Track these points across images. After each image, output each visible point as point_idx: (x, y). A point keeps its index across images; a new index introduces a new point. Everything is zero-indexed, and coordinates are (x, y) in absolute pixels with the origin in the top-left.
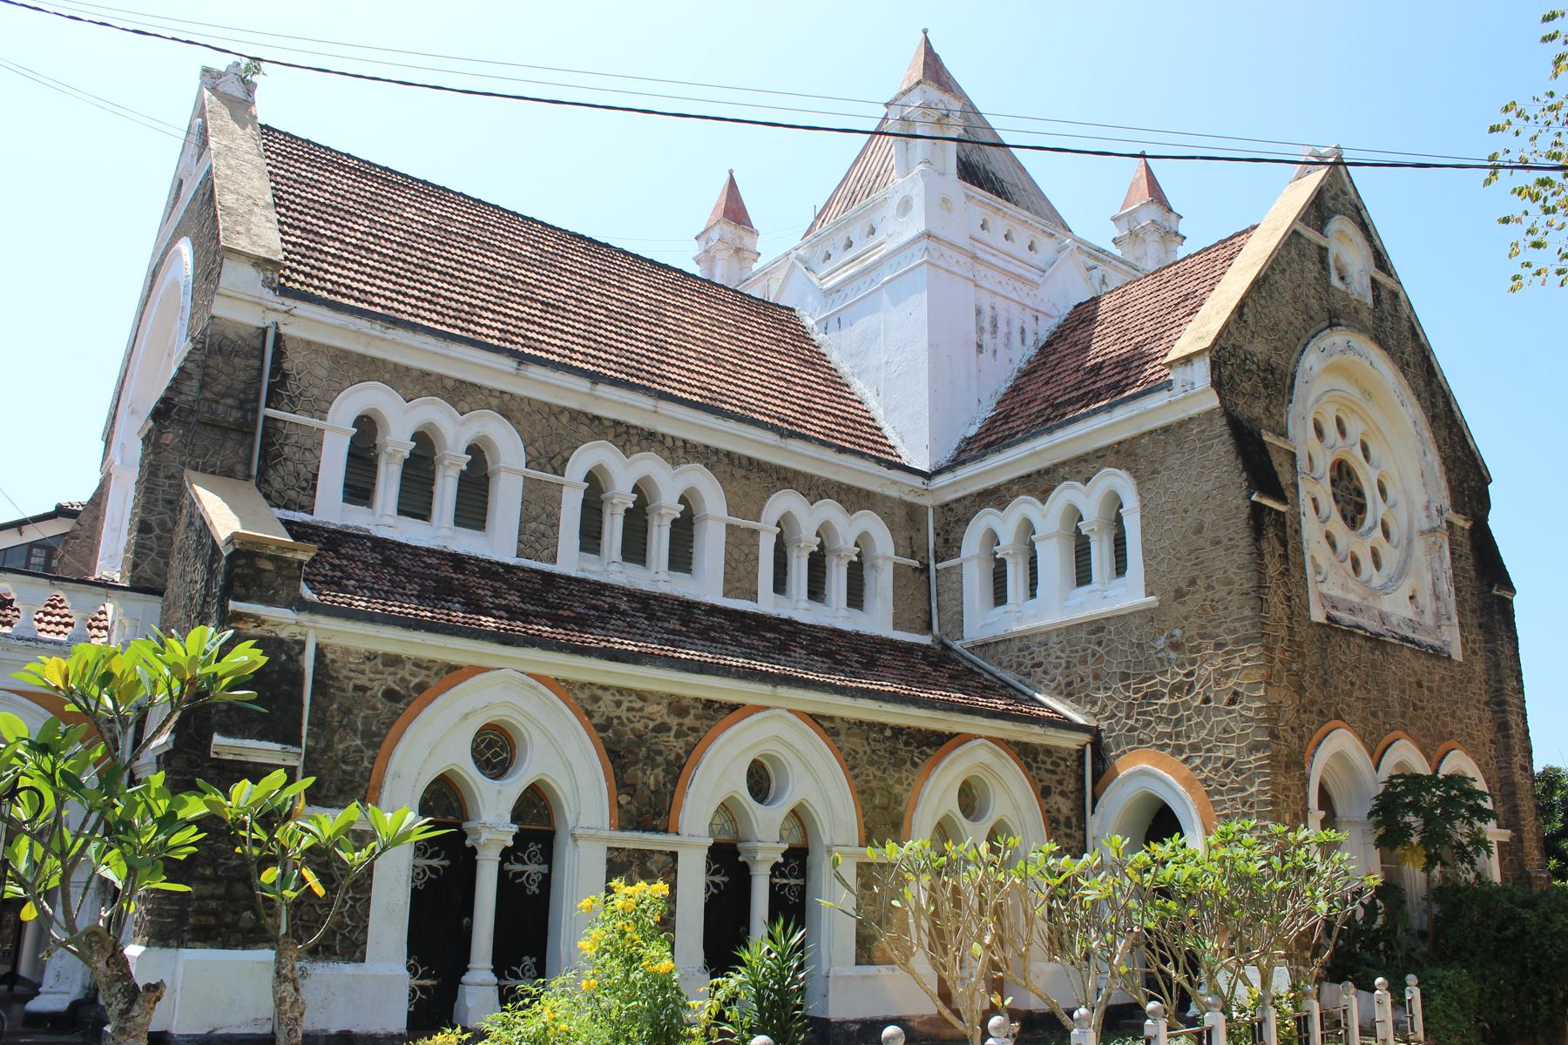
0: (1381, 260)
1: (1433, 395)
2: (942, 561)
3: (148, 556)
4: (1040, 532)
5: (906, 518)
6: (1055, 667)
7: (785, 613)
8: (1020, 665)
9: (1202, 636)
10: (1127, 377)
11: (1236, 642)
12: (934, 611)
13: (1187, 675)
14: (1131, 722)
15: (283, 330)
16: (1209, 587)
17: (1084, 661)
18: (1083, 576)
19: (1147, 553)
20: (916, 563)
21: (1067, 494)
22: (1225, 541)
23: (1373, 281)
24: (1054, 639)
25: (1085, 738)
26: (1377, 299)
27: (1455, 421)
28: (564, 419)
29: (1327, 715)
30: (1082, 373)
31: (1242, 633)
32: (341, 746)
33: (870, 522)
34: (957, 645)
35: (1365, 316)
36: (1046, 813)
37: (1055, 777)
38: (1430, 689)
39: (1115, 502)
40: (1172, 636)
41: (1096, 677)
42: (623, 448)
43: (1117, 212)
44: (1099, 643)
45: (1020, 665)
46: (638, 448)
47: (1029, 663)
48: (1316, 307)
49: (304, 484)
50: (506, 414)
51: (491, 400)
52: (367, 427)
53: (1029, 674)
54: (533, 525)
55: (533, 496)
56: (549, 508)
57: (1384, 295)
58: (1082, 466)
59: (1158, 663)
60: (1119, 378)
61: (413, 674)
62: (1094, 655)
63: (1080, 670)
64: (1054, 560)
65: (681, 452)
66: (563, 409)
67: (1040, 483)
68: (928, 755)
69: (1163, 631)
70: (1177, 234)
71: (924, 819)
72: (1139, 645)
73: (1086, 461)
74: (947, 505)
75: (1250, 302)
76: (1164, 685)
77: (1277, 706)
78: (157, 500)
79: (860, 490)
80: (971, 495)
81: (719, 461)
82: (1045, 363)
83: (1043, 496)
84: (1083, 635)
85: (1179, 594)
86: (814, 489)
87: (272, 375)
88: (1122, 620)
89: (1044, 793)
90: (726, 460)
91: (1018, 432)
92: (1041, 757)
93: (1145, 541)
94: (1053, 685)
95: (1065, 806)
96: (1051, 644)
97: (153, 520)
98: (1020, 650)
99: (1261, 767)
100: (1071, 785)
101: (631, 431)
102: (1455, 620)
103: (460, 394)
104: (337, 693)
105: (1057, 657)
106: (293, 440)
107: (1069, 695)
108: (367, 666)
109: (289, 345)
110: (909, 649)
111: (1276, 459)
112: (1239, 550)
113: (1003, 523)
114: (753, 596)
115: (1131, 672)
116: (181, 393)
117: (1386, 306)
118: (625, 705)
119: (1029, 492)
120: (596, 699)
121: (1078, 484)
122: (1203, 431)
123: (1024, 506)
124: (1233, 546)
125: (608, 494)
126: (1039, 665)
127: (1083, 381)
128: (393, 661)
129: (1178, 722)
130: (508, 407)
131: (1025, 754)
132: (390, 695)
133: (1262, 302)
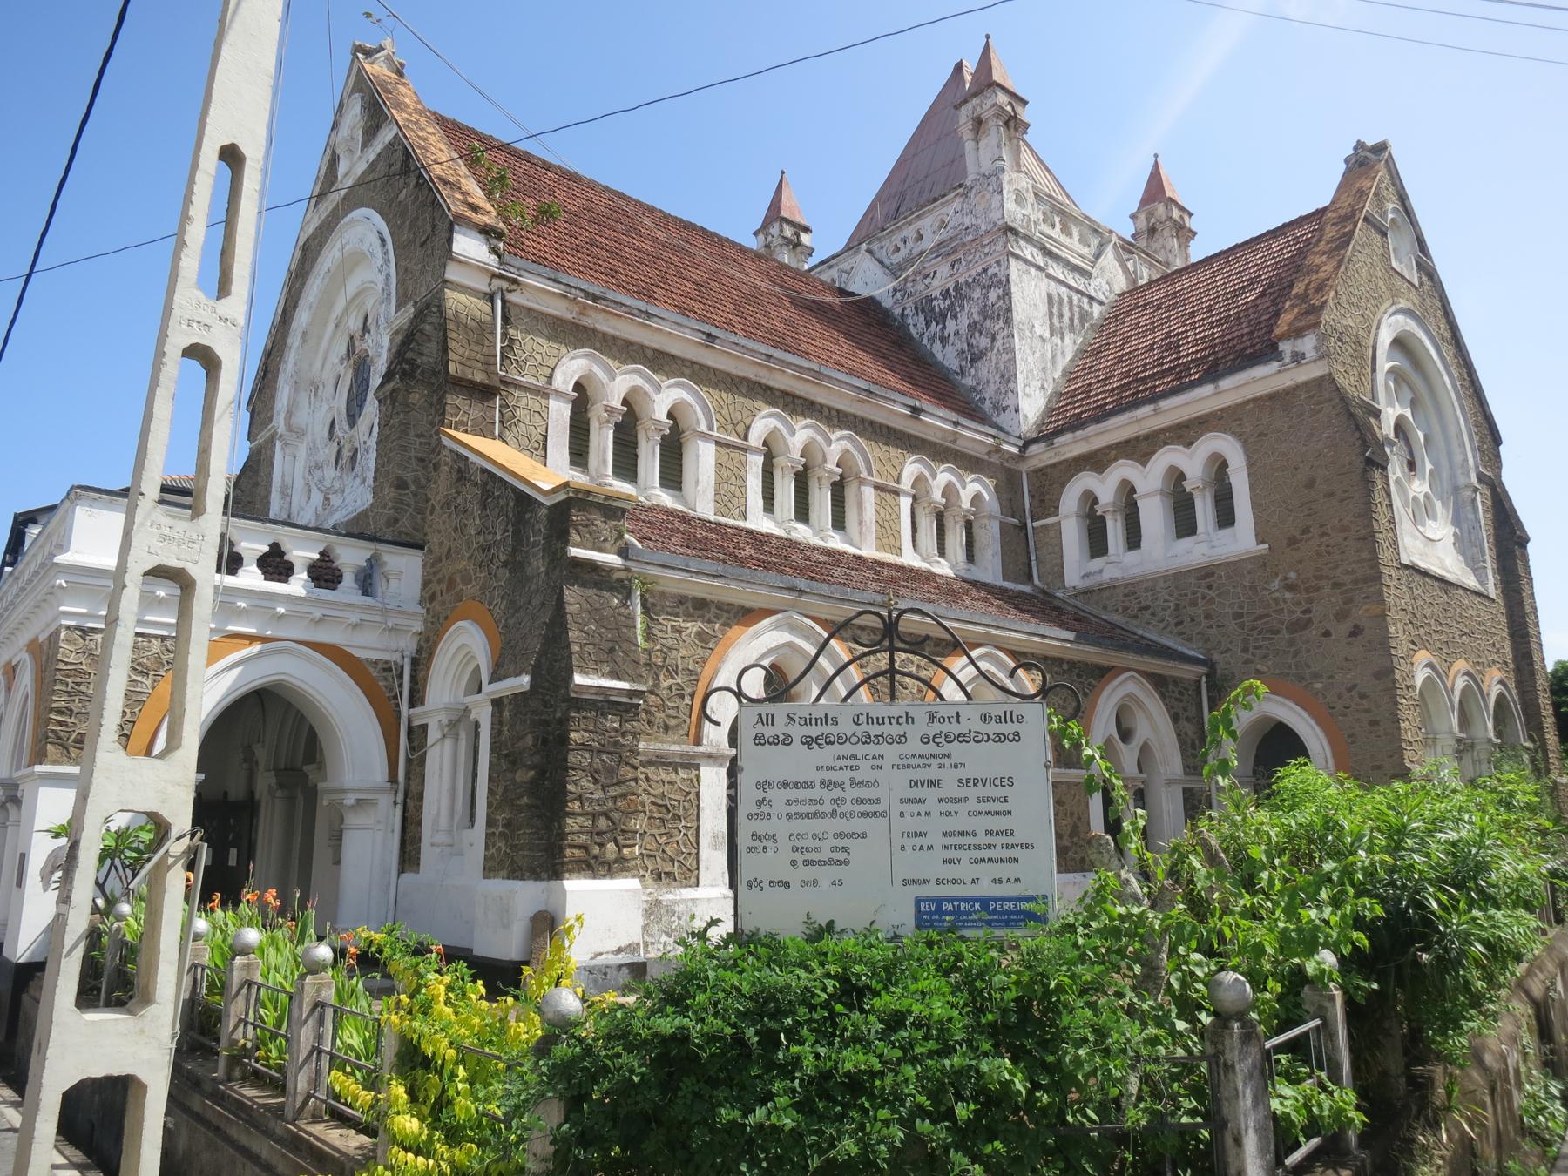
3: (406, 511)
4: (1141, 488)
5: (1008, 483)
6: (1164, 609)
7: (924, 566)
8: (1126, 609)
9: (1320, 578)
11: (1355, 582)
12: (1034, 563)
13: (1304, 612)
14: (1246, 656)
15: (509, 297)
17: (1194, 603)
18: (1185, 525)
19: (1257, 506)
20: (1015, 521)
24: (1162, 585)
25: (1203, 670)
36: (1178, 735)
37: (1181, 705)
39: (1219, 467)
40: (1286, 579)
44: (1210, 587)
47: (1134, 605)
48: (1384, 288)
49: (536, 445)
51: (684, 369)
53: (1136, 617)
58: (1185, 433)
59: (1273, 604)
64: (1154, 515)
65: (836, 420)
66: (743, 379)
67: (1140, 449)
68: (1094, 687)
69: (1277, 575)
70: (1190, 231)
72: (1253, 589)
74: (1041, 470)
78: (410, 458)
79: (971, 456)
80: (1066, 460)
81: (865, 429)
83: (1143, 458)
84: (1193, 580)
85: (1292, 542)
87: (502, 342)
88: (1233, 568)
89: (1175, 719)
90: (870, 430)
92: (1171, 687)
94: (1162, 625)
95: (1190, 729)
96: (1158, 589)
97: (408, 476)
100: (1192, 712)
103: (661, 362)
104: (659, 634)
105: (1165, 601)
106: (523, 403)
107: (1180, 634)
109: (513, 311)
113: (1105, 487)
114: (898, 550)
115: (1245, 611)
116: (422, 354)
119: (1128, 457)
121: (1181, 448)
123: (1125, 469)
126: (1147, 608)
127: (1162, 358)
131: (1160, 683)
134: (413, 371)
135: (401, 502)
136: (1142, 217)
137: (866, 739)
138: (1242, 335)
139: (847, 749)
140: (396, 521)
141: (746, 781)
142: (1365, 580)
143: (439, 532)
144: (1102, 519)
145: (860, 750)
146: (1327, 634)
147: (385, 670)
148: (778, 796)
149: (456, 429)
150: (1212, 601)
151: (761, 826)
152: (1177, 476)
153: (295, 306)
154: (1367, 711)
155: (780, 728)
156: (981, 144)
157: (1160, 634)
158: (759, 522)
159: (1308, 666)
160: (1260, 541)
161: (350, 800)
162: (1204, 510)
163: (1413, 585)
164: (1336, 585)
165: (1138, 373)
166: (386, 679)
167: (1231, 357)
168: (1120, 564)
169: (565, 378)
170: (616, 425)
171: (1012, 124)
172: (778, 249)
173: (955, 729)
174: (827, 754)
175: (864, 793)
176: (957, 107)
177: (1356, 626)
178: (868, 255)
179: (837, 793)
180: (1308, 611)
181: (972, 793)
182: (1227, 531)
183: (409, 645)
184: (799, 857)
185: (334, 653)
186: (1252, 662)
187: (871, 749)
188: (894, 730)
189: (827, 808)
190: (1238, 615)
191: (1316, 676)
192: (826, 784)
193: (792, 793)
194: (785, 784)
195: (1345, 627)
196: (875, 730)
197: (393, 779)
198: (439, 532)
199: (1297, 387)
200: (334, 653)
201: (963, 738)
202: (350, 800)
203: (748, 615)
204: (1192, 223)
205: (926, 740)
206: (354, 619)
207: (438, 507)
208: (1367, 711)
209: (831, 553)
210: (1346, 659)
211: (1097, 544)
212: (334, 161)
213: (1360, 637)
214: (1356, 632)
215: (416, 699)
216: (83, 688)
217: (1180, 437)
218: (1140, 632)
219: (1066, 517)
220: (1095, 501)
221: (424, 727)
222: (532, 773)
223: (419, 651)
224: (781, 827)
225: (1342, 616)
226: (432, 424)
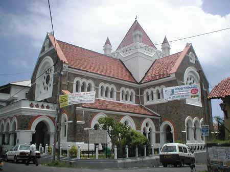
0: (196, 57)
5: (137, 90)
18: (159, 98)
33: (132, 90)
52: (77, 82)
64: (155, 96)
67: (154, 86)
71: (142, 128)
83: (154, 88)
103: (88, 78)
123: (152, 89)
128: (91, 112)
130: (93, 79)
131: (153, 119)
132: (91, 116)
152: (158, 91)
168: (151, 103)
169: (75, 81)
185: (49, 116)
200: (49, 116)
204: (170, 47)
209: (110, 102)
225: (176, 111)
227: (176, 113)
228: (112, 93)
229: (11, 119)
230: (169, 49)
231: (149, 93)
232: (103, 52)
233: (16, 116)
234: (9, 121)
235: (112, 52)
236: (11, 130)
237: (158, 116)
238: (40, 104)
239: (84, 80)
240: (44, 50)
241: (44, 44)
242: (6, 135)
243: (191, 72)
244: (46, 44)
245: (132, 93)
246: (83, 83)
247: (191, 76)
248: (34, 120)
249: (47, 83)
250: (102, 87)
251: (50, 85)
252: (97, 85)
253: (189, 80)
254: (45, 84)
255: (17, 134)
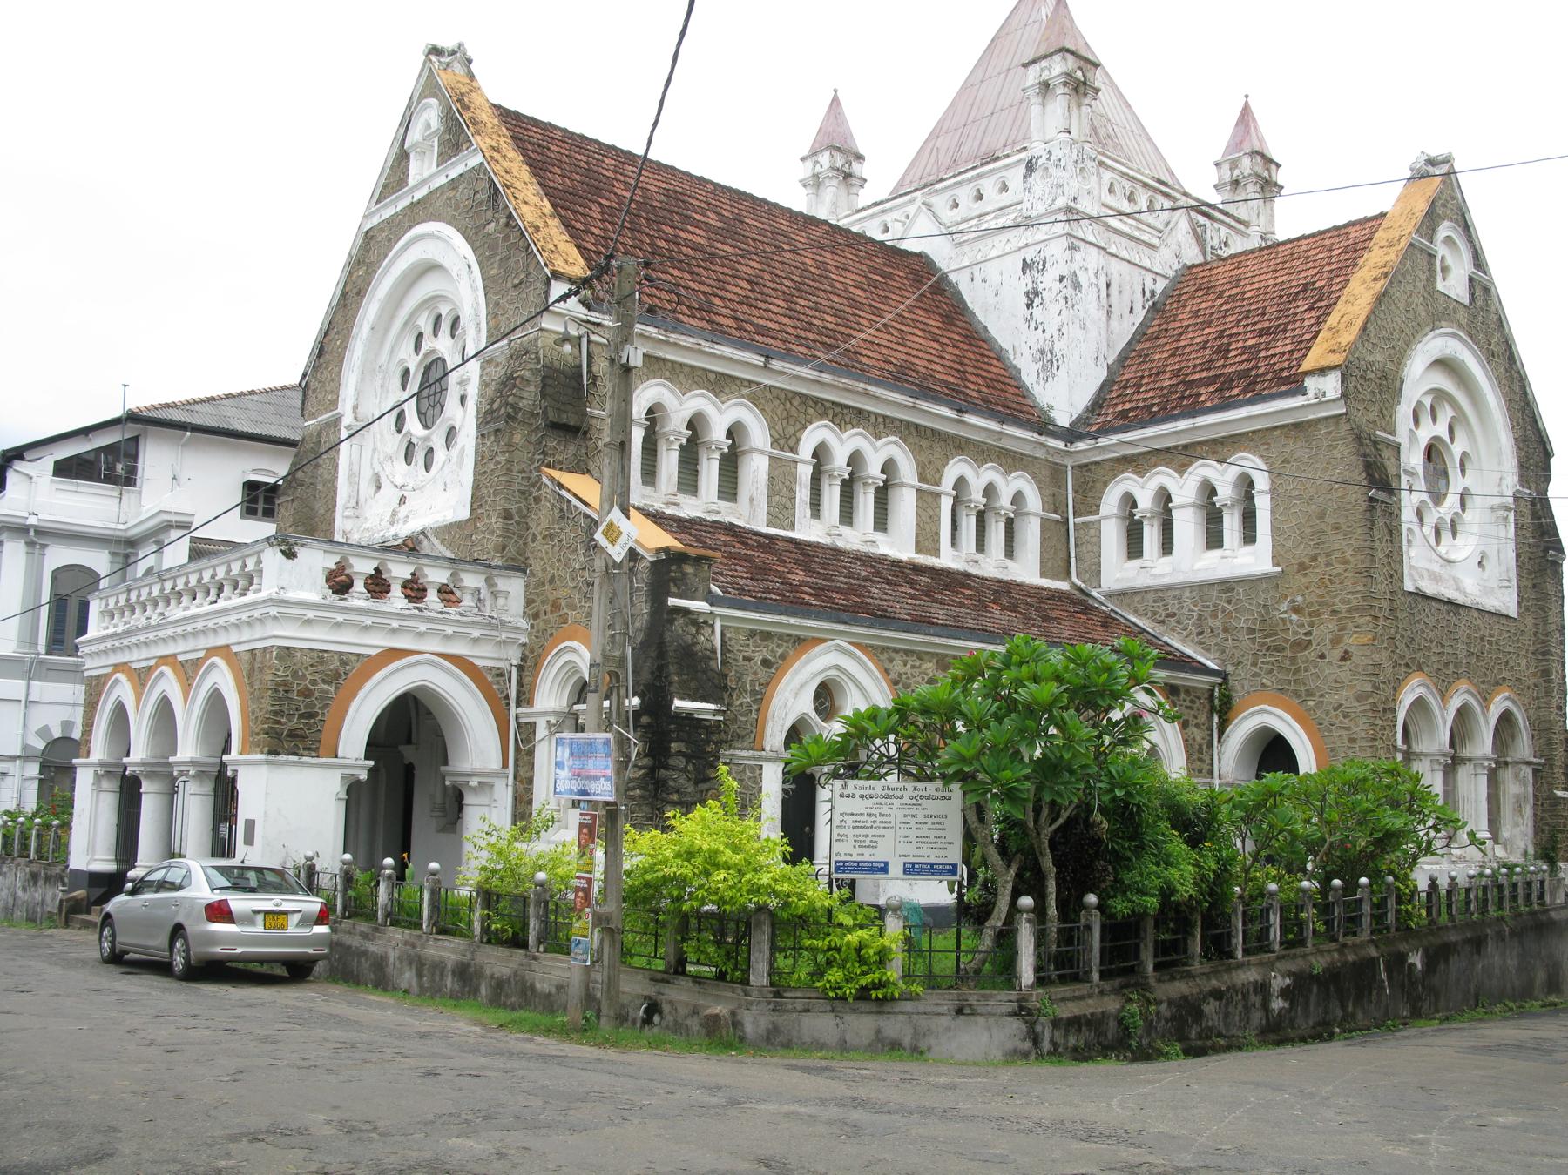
1: (1512, 379)
2: (1080, 516)
4: (1176, 500)
5: (1051, 477)
8: (1155, 613)
9: (1321, 603)
10: (1258, 368)
11: (1349, 611)
12: (1073, 561)
13: (1305, 634)
14: (1255, 670)
15: (593, 338)
16: (1328, 564)
18: (1214, 539)
20: (1057, 517)
21: (1206, 469)
22: (1344, 527)
23: (1471, 279)
24: (1187, 594)
25: (1218, 680)
26: (1472, 297)
27: (1528, 403)
28: (796, 402)
29: (1413, 666)
30: (1208, 352)
31: (1354, 603)
32: (738, 702)
33: (1021, 482)
34: (1094, 593)
35: (1462, 316)
36: (1186, 741)
38: (1490, 643)
41: (1225, 630)
42: (839, 426)
43: (1218, 158)
44: (1229, 602)
45: (1155, 613)
46: (849, 426)
48: (1423, 314)
50: (754, 399)
53: (1162, 622)
54: (777, 498)
55: (777, 472)
56: (788, 483)
57: (1478, 292)
58: (1218, 448)
60: (1244, 366)
61: (778, 646)
62: (1223, 611)
63: (1211, 622)
64: (1187, 526)
67: (1181, 456)
69: (1286, 597)
70: (1276, 184)
73: (1222, 443)
75: (1373, 317)
76: (1286, 641)
77: (1377, 665)
82: (1166, 330)
83: (1181, 469)
84: (1215, 593)
85: (1302, 567)
86: (981, 453)
90: (915, 433)
91: (1153, 405)
92: (1183, 696)
93: (1273, 520)
94: (1185, 633)
97: (513, 507)
98: (1155, 601)
99: (1365, 711)
101: (845, 411)
102: (1514, 583)
103: (720, 384)
108: (751, 642)
110: (1057, 596)
111: (1386, 453)
112: (1355, 536)
115: (1257, 627)
116: (522, 398)
117: (1479, 303)
118: (909, 666)
119: (1167, 465)
120: (891, 660)
122: (1330, 433)
123: (1163, 477)
124: (1351, 532)
125: (828, 467)
126: (1173, 615)
127: (1211, 361)
128: (766, 636)
129: (1297, 670)
133: (1382, 315)
134: (516, 413)
135: (507, 530)
136: (1226, 167)
137: (887, 797)
138: (1283, 354)
139: (878, 801)
140: (504, 548)
141: (836, 812)
142: (1357, 609)
143: (542, 559)
144: (1140, 523)
145: (884, 801)
146: (1322, 656)
147: (498, 675)
148: (849, 819)
149: (554, 468)
150: (1230, 613)
151: (842, 831)
152: (1209, 490)
153: (361, 293)
154: (1348, 729)
155: (850, 791)
156: (1049, 108)
157: (1183, 641)
158: (809, 531)
159: (1305, 684)
160: (1276, 564)
161: (474, 782)
162: (1231, 525)
163: (1415, 611)
164: (1334, 612)
165: (1187, 375)
166: (498, 683)
167: (1269, 376)
168: (1155, 570)
170: (681, 446)
171: (1082, 89)
172: (827, 181)
173: (924, 794)
174: (869, 803)
175: (884, 819)
176: (1025, 65)
177: (1346, 652)
178: (923, 207)
179: (873, 818)
180: (1309, 633)
181: (929, 820)
182: (1249, 549)
183: (514, 656)
184: (857, 844)
186: (1259, 675)
187: (888, 801)
188: (899, 793)
189: (869, 824)
190: (1251, 631)
191: (1310, 694)
192: (869, 815)
193: (855, 818)
194: (852, 814)
195: (1338, 653)
196: (890, 793)
197: (505, 765)
198: (542, 559)
199: (1319, 420)
201: (927, 798)
202: (474, 782)
203: (802, 643)
204: (1281, 177)
205: (912, 798)
206: (476, 634)
207: (539, 537)
208: (1348, 729)
210: (1336, 682)
211: (1134, 547)
212: (401, 158)
213: (1348, 663)
214: (1346, 657)
215: (524, 698)
216: (290, 695)
217: (1215, 453)
218: (1165, 639)
219: (1106, 517)
220: (1134, 505)
221: (532, 725)
222: (642, 772)
223: (524, 658)
224: (850, 832)
225: (1336, 641)
226: (532, 460)
227: (1334, 655)
228: (883, 496)
229: (188, 671)
230: (1269, 188)
231: (1145, 501)
232: (796, 199)
233: (223, 651)
234: (169, 685)
235: (865, 197)
236: (188, 749)
237: (1205, 670)
238: (399, 571)
239: (699, 401)
240: (402, 182)
241: (406, 123)
242: (146, 786)
243: (1443, 364)
244: (415, 135)
245: (1018, 498)
246: (691, 425)
247: (1439, 395)
248: (368, 676)
249: (426, 422)
250: (820, 453)
251: (451, 433)
252: (785, 440)
253: (1426, 419)
254: (413, 424)
255: (241, 785)
